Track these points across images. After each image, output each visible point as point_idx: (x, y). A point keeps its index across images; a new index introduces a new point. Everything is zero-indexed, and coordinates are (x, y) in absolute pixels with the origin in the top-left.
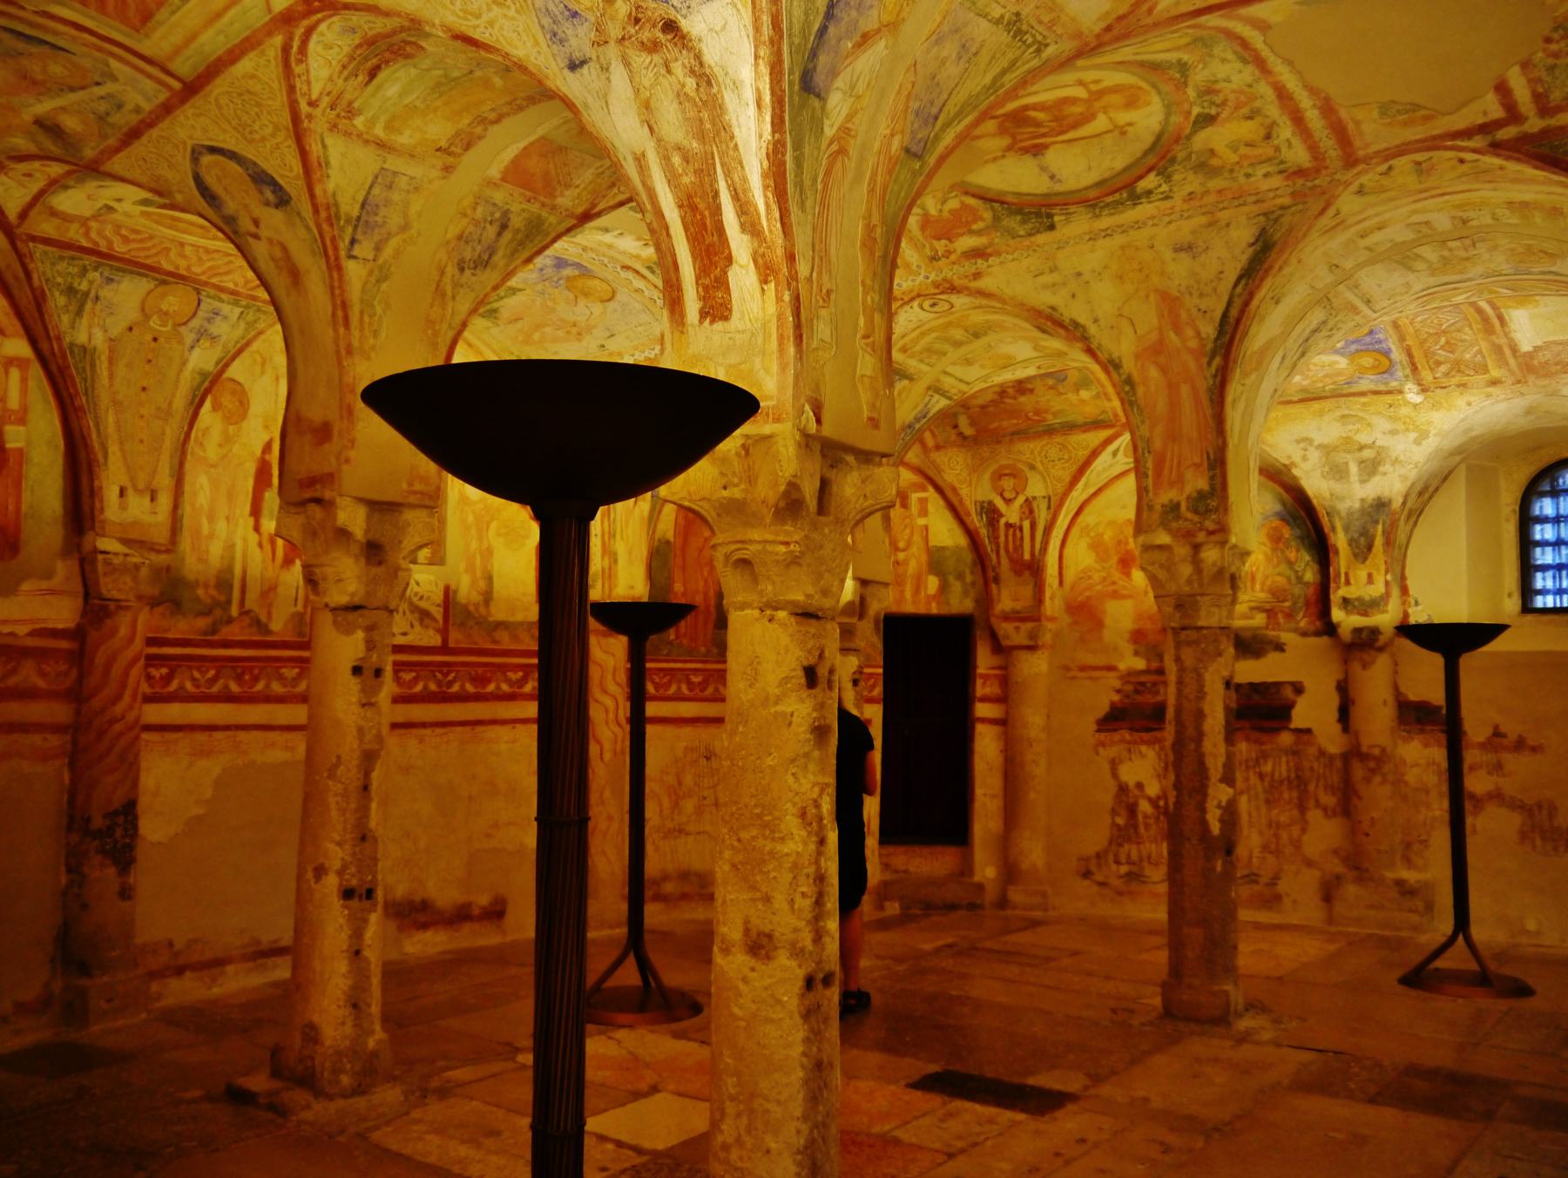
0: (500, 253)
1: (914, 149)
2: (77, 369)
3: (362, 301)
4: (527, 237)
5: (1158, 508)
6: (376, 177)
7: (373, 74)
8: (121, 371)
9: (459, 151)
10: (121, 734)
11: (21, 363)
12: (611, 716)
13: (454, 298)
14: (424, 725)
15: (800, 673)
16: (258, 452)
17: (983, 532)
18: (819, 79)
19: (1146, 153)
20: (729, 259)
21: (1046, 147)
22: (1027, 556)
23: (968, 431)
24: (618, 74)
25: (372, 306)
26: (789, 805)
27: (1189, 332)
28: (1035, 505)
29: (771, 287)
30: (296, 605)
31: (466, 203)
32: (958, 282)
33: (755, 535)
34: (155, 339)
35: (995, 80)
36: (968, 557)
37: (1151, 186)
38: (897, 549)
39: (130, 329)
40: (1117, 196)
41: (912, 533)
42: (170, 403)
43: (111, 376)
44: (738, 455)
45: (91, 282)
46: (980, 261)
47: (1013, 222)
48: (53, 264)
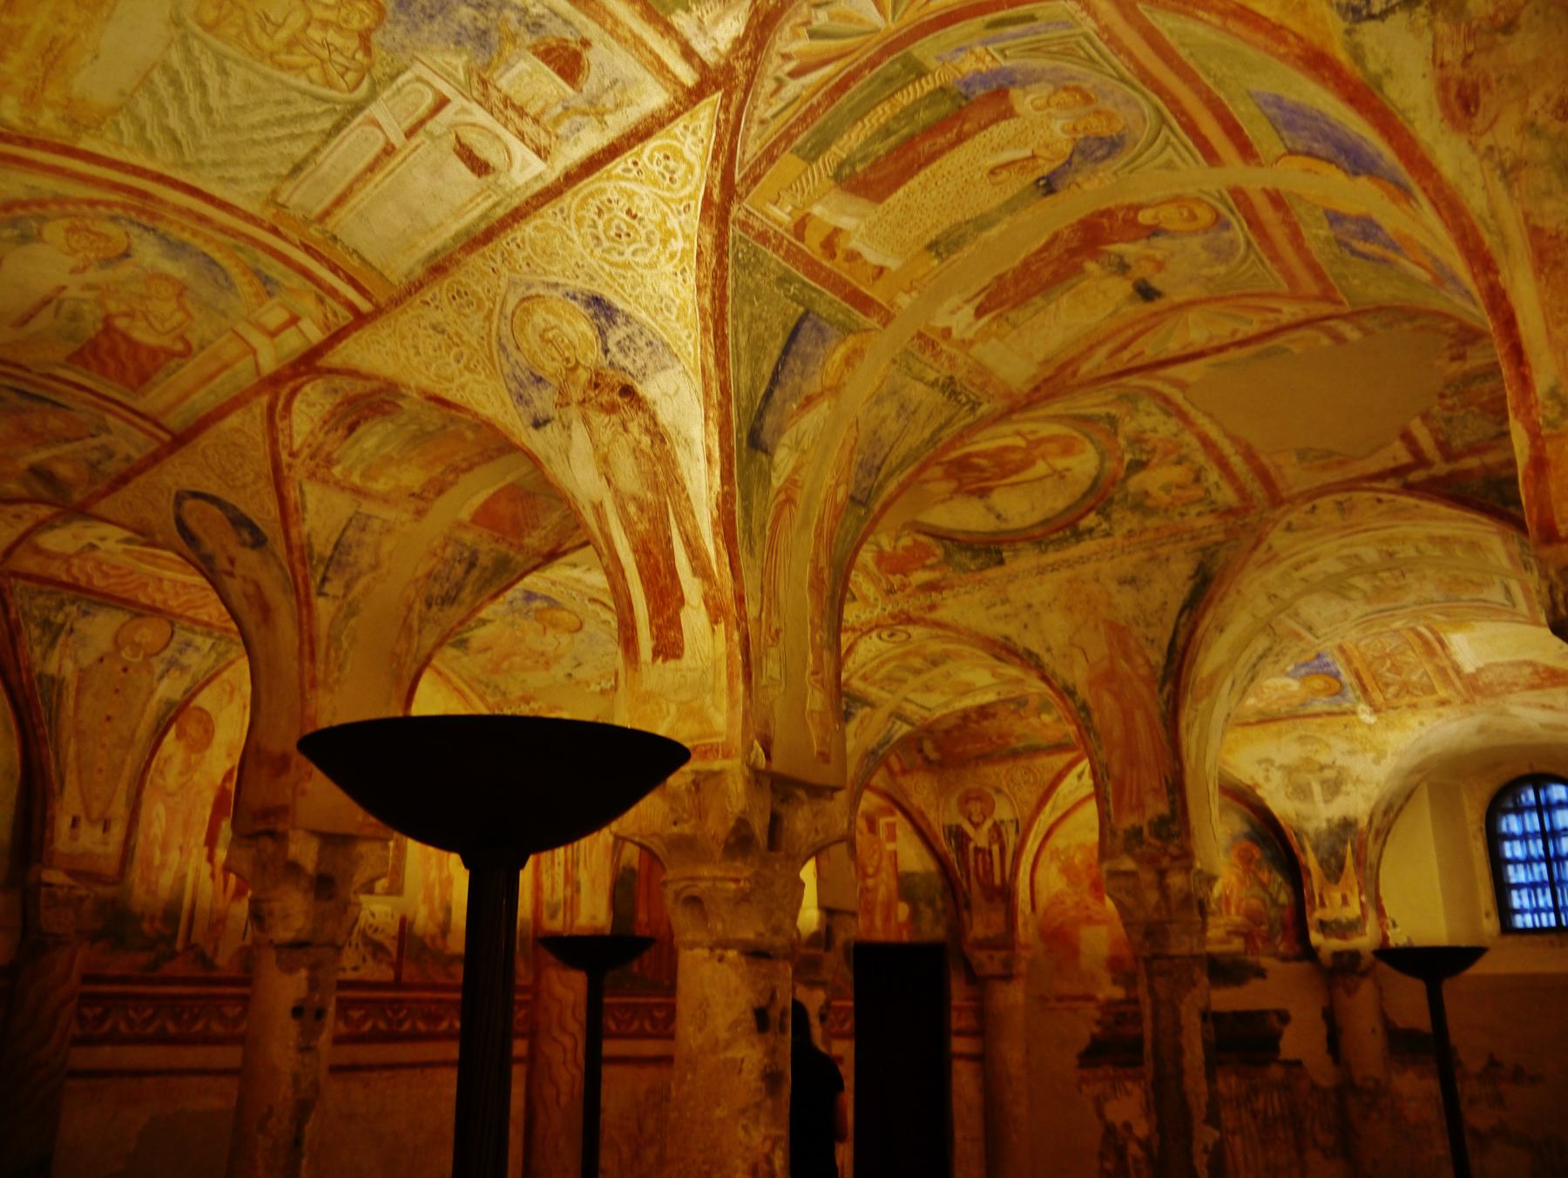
0: (468, 590)
1: (859, 497)
3: (329, 636)
5: (1120, 833)
6: (351, 520)
7: (352, 428)
8: (88, 700)
9: (431, 495)
12: (569, 1057)
13: (420, 632)
14: (370, 1068)
15: (750, 1016)
16: (219, 781)
17: (953, 856)
18: (766, 436)
19: (1085, 495)
20: (681, 601)
21: (991, 489)
22: (997, 881)
23: (934, 755)
24: (579, 432)
26: (739, 1162)
27: (1139, 661)
28: (1003, 829)
29: (721, 627)
31: (436, 543)
32: (914, 614)
33: (705, 871)
34: (125, 670)
35: (933, 435)
36: (938, 882)
37: (1093, 524)
38: (865, 876)
39: (101, 660)
40: (1061, 534)
41: (881, 858)
43: (77, 706)
44: (688, 790)
45: (67, 616)
46: (934, 594)
47: (964, 558)
48: (31, 598)
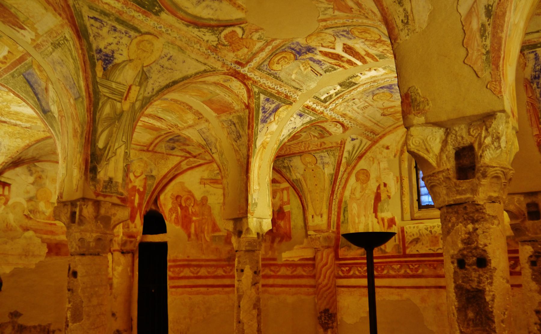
1: (77, 96)
3: (221, 163)
4: (241, 123)
8: (308, 182)
10: (321, 288)
11: (287, 189)
13: (240, 150)
16: (375, 191)
18: (46, 108)
25: (224, 163)
30: (395, 242)
31: (220, 125)
34: (313, 170)
35: (72, 58)
42: (324, 186)
43: (307, 185)
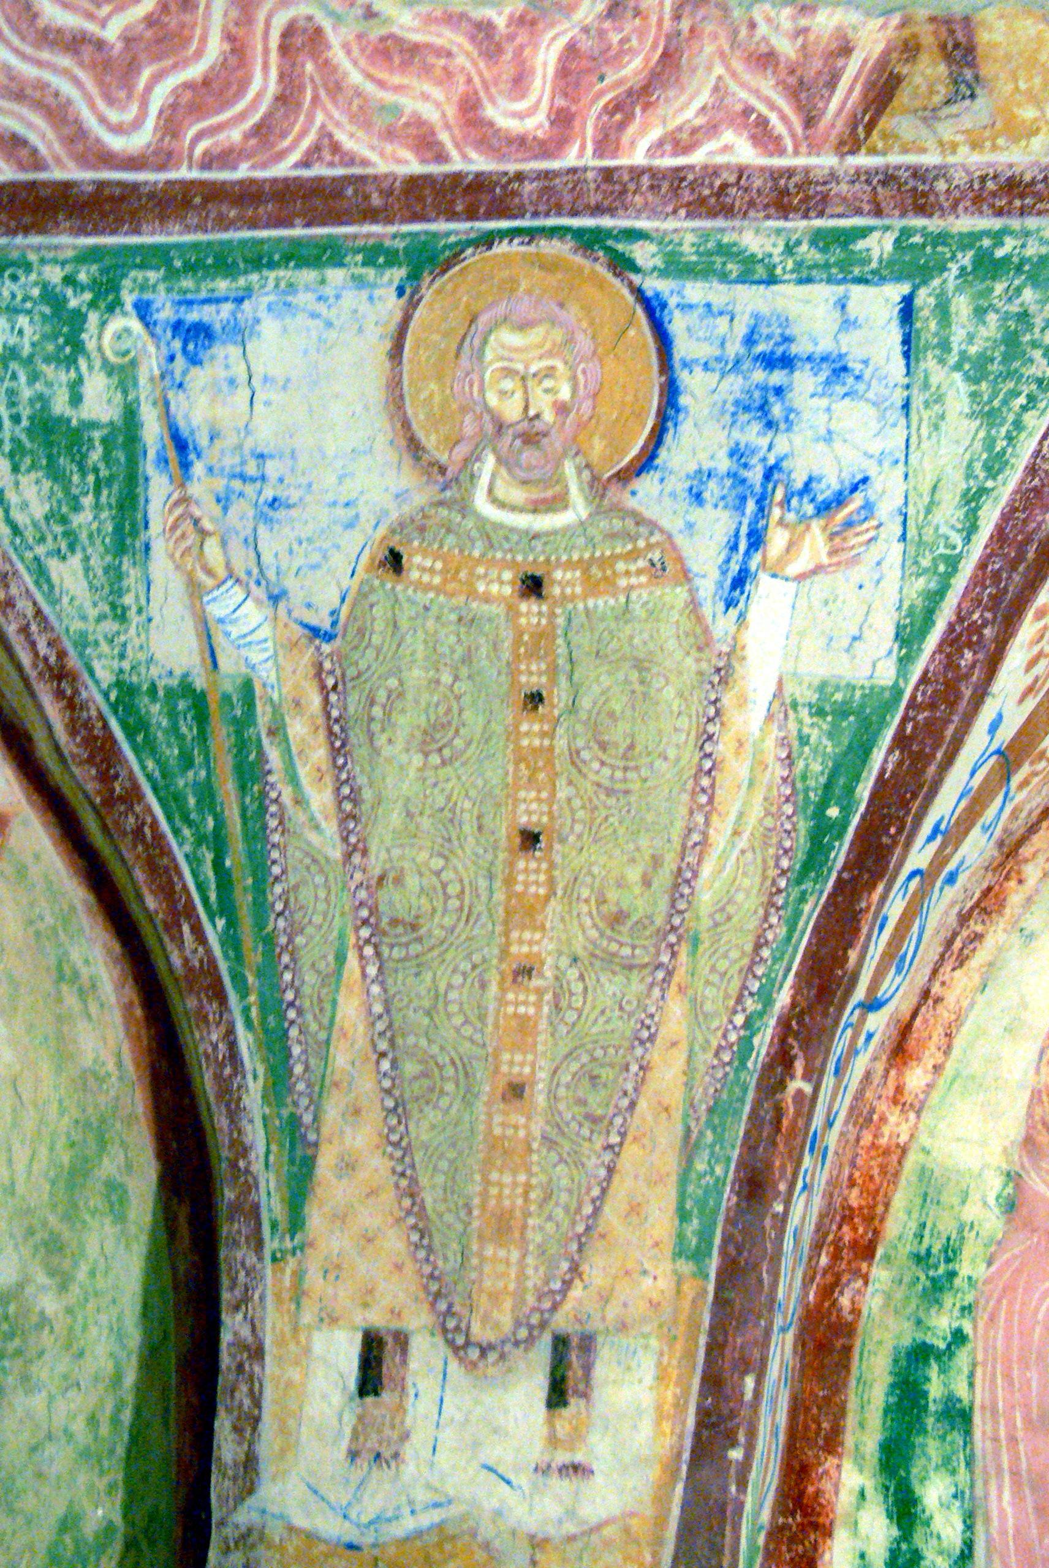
2: (172, 801)
34: (533, 586)
